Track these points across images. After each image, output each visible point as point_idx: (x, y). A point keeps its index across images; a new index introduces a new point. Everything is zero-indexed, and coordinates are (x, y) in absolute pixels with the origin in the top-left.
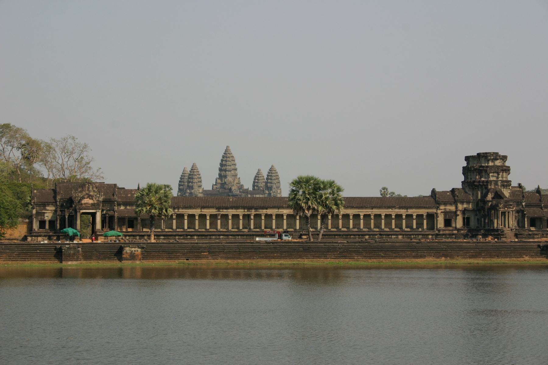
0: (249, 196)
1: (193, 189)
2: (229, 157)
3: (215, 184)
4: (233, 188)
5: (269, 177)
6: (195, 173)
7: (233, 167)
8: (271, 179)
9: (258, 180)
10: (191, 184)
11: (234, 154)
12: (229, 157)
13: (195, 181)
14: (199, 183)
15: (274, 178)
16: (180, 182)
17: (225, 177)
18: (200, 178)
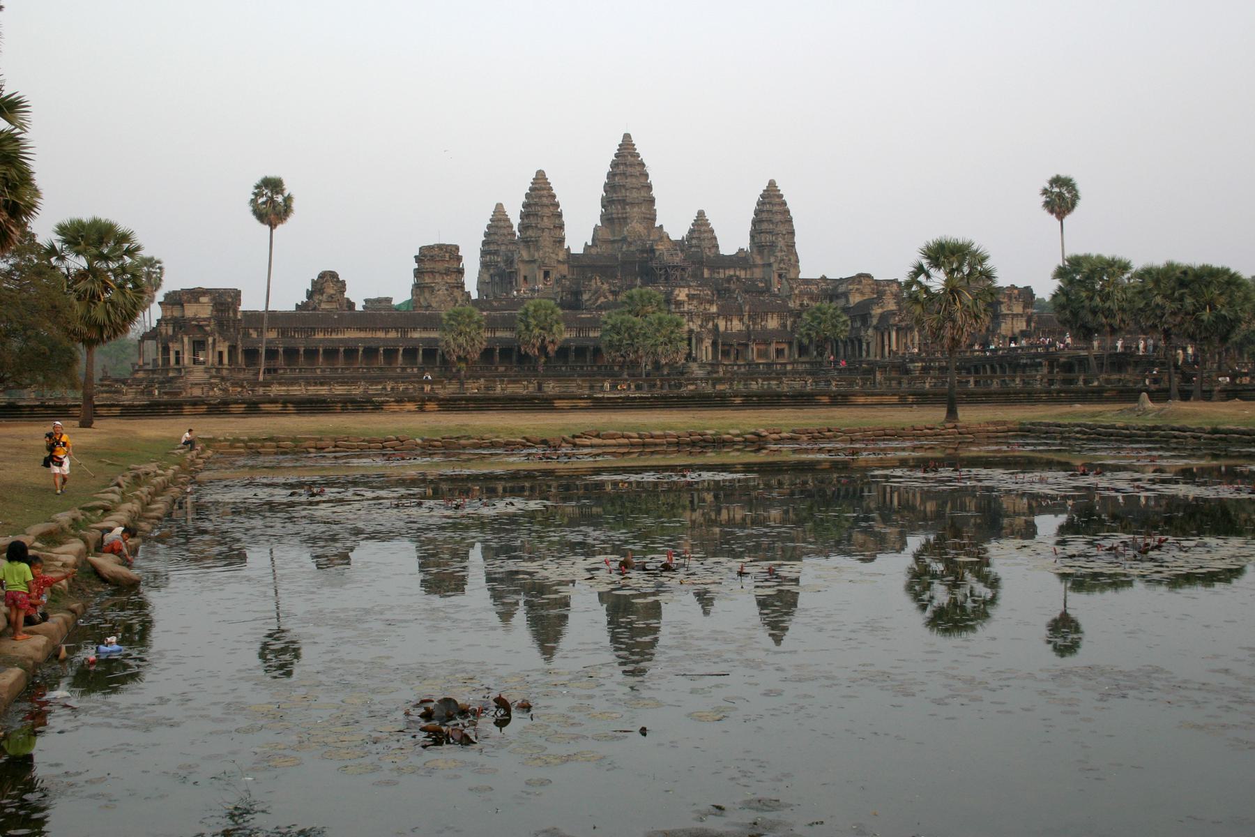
0: (706, 273)
1: (538, 249)
2: (632, 165)
3: (590, 243)
4: (660, 247)
5: (764, 216)
6: (545, 201)
7: (643, 193)
8: (770, 221)
9: (699, 238)
10: (530, 233)
11: (645, 156)
12: (632, 165)
13: (546, 222)
14: (557, 232)
15: (779, 217)
16: (484, 243)
17: (624, 220)
18: (560, 215)
